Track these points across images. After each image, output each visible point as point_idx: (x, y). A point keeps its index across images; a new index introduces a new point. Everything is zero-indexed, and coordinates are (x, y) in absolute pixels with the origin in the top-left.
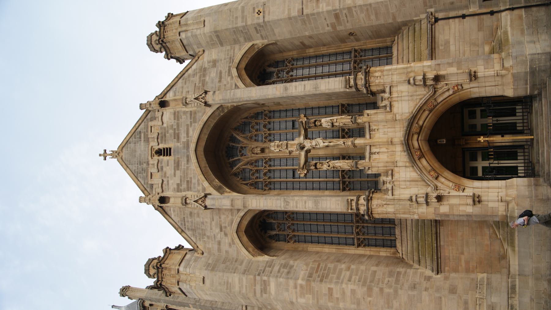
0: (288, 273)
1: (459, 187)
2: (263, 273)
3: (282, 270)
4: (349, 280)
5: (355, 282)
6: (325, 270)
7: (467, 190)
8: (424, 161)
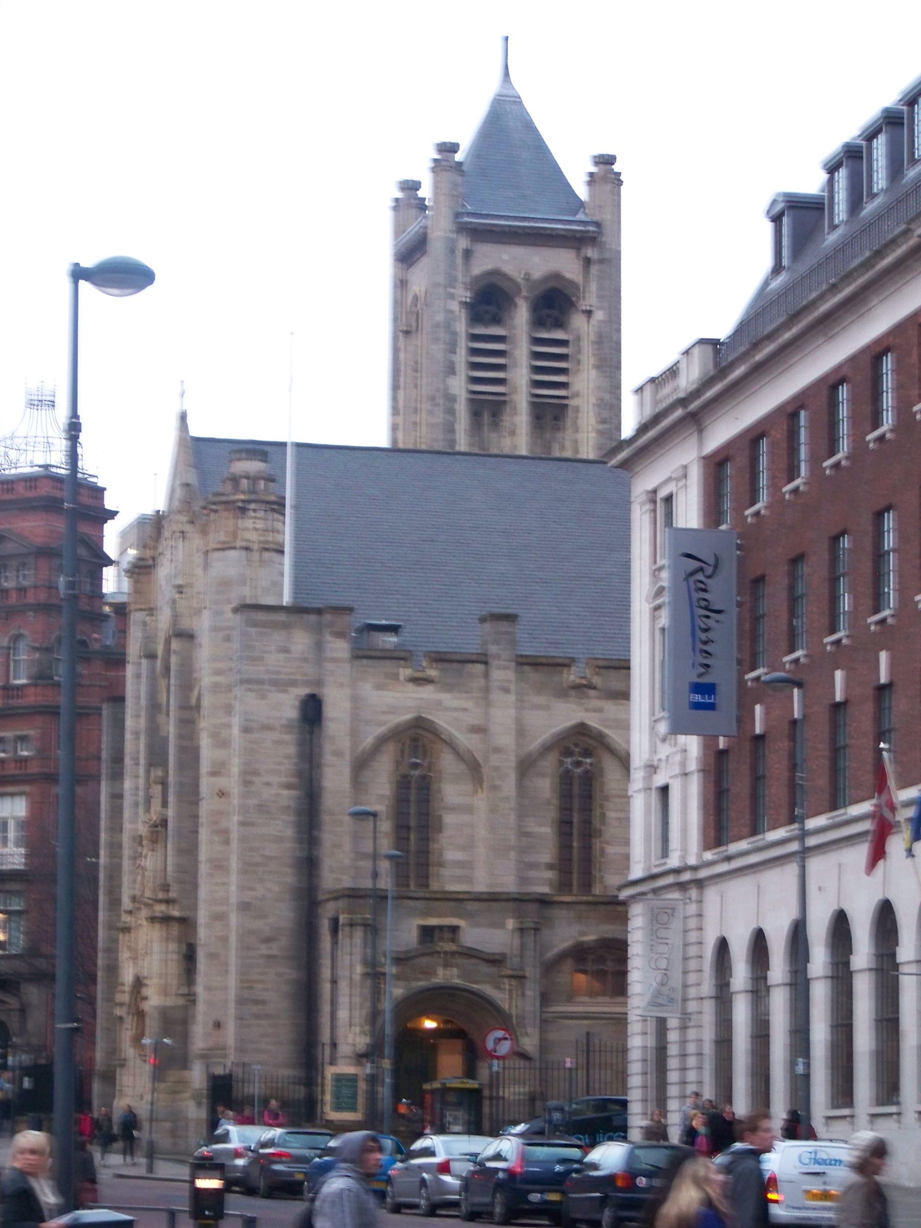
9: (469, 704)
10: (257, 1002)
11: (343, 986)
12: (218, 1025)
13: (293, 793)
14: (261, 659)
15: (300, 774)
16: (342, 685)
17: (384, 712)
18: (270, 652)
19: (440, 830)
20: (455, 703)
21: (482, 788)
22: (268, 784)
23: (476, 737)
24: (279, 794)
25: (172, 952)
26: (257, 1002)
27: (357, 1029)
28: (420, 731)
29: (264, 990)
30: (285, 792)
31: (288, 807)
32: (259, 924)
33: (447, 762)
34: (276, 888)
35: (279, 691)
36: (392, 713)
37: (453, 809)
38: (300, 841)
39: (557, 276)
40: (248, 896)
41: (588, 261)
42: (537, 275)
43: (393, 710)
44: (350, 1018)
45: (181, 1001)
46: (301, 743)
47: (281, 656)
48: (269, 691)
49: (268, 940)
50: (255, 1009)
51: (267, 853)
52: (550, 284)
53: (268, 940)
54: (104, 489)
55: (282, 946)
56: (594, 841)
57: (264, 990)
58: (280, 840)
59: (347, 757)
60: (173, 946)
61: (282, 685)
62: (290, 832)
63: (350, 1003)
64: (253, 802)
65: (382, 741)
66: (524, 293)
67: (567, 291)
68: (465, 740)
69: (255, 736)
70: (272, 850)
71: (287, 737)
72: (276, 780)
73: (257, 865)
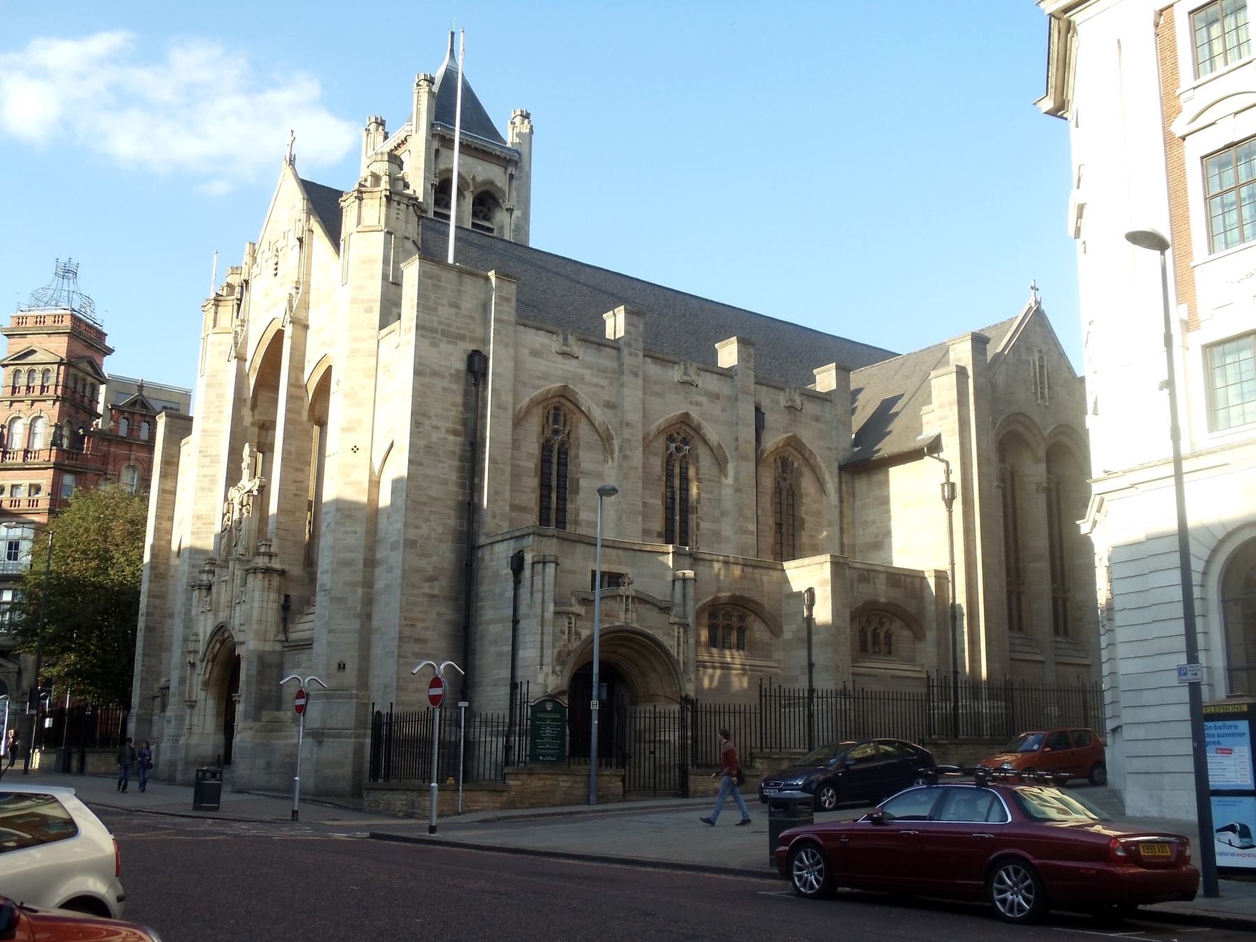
0: (203, 489)
1: (206, 684)
2: (204, 456)
3: (207, 480)
4: (193, 566)
5: (192, 572)
6: (206, 533)
7: (203, 693)
8: (218, 645)
9: (605, 383)
10: (418, 641)
11: (529, 627)
12: (341, 667)
13: (460, 439)
14: (436, 309)
15: (464, 422)
16: (507, 346)
17: (539, 378)
18: (443, 305)
19: (577, 491)
20: (595, 380)
21: (612, 458)
22: (437, 428)
23: (609, 412)
24: (446, 439)
25: (273, 602)
26: (418, 641)
27: (548, 669)
28: (563, 401)
29: (426, 629)
30: (451, 438)
31: (454, 453)
32: (423, 563)
33: (583, 432)
34: (440, 530)
35: (450, 342)
36: (545, 379)
37: (587, 474)
38: (463, 486)
39: (492, 183)
40: (412, 533)
41: (511, 176)
42: (479, 179)
43: (545, 377)
44: (542, 657)
45: (278, 647)
46: (466, 394)
47: (453, 311)
48: (441, 341)
49: (431, 579)
50: (416, 648)
51: (434, 494)
52: (487, 188)
53: (431, 579)
54: (106, 335)
55: (441, 586)
56: (690, 516)
57: (426, 629)
58: (445, 482)
59: (510, 412)
60: (273, 596)
61: (455, 338)
62: (453, 476)
63: (542, 642)
64: (423, 442)
65: (535, 403)
66: (471, 189)
67: (497, 195)
68: (598, 414)
69: (427, 380)
70: (436, 491)
71: (455, 387)
72: (443, 425)
73: (425, 504)
